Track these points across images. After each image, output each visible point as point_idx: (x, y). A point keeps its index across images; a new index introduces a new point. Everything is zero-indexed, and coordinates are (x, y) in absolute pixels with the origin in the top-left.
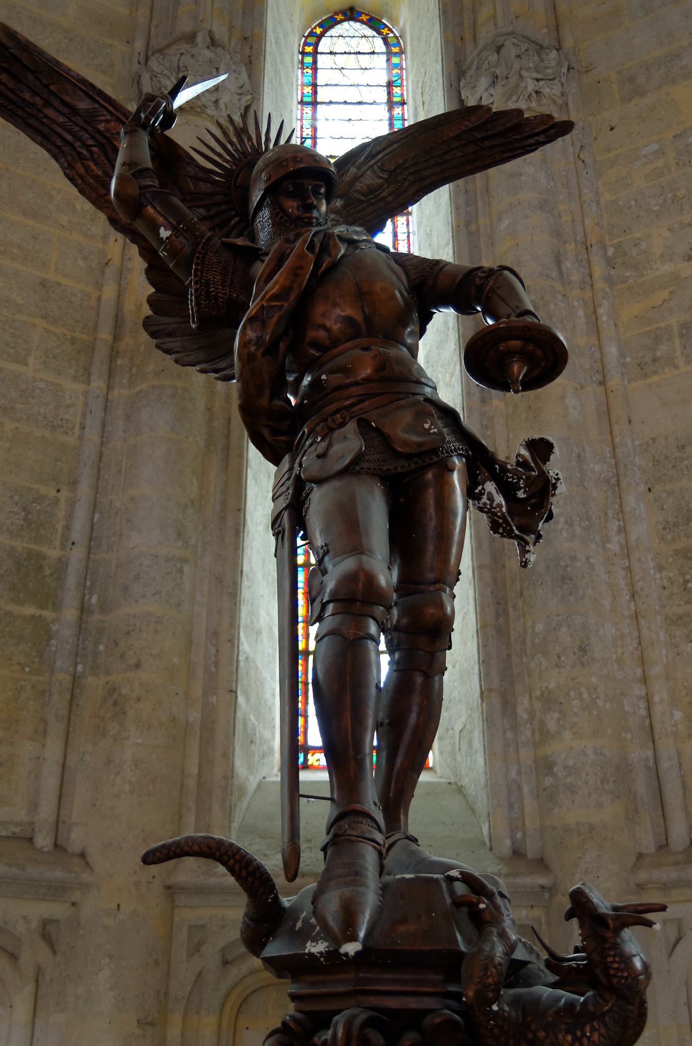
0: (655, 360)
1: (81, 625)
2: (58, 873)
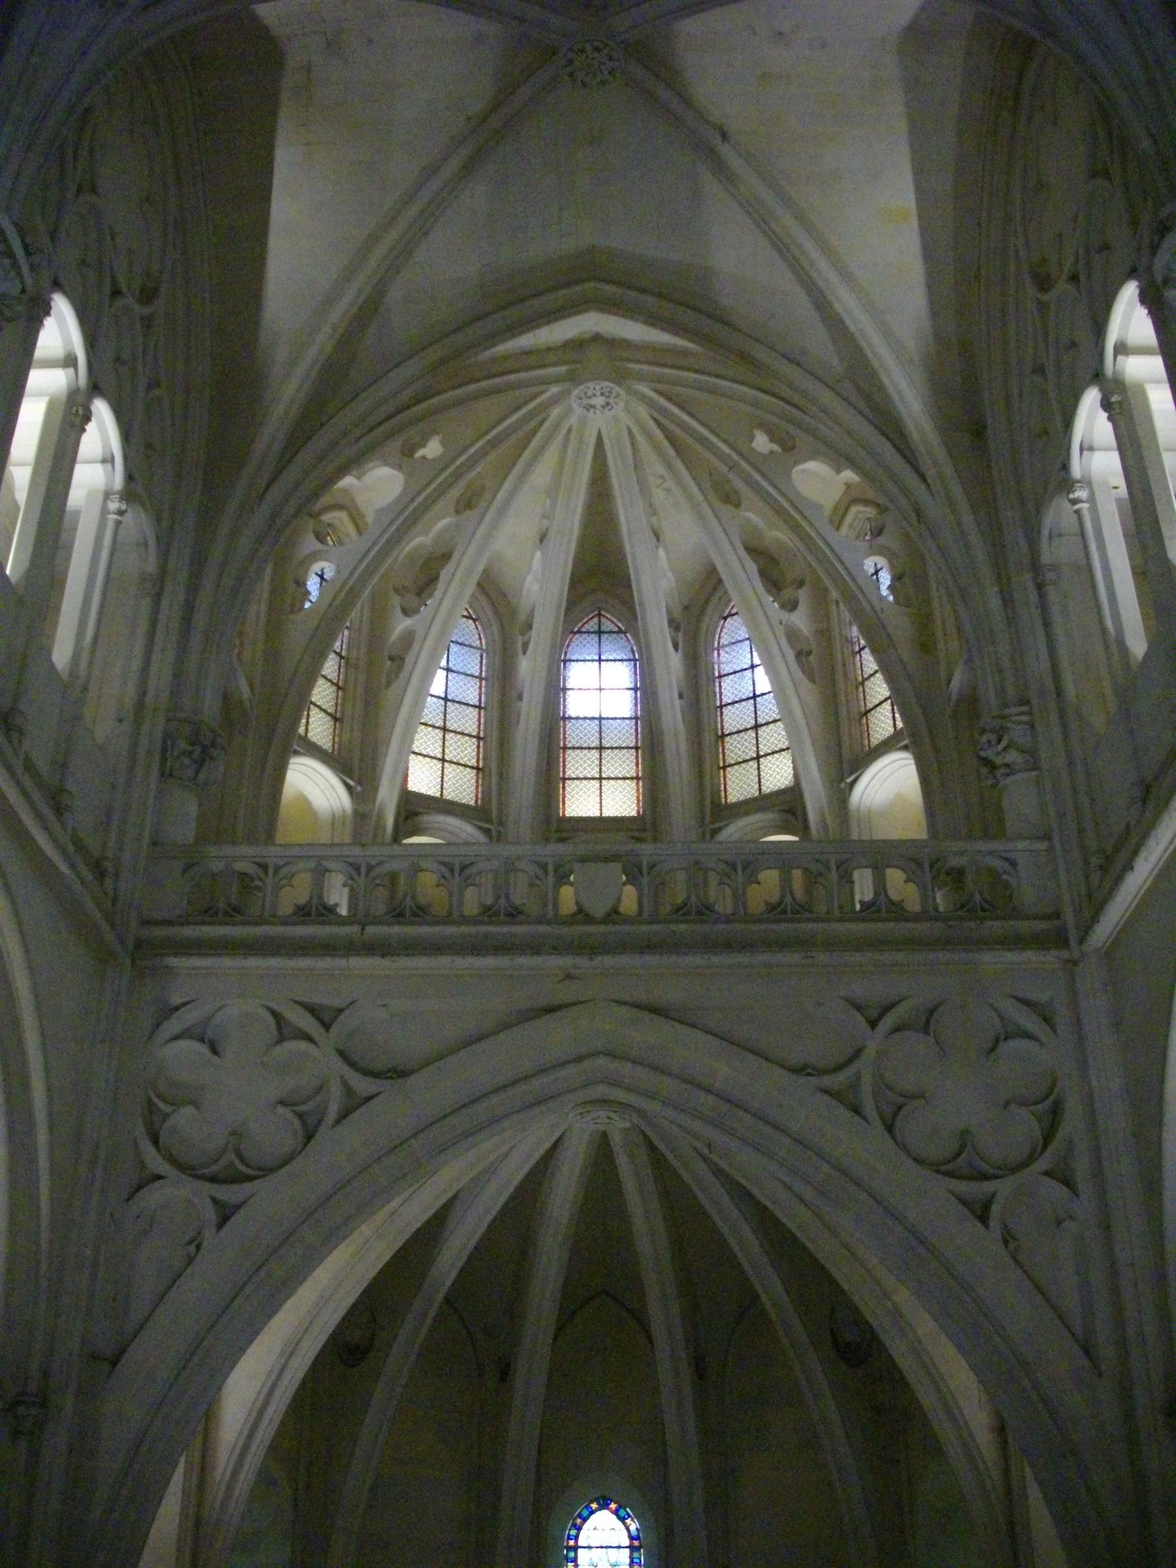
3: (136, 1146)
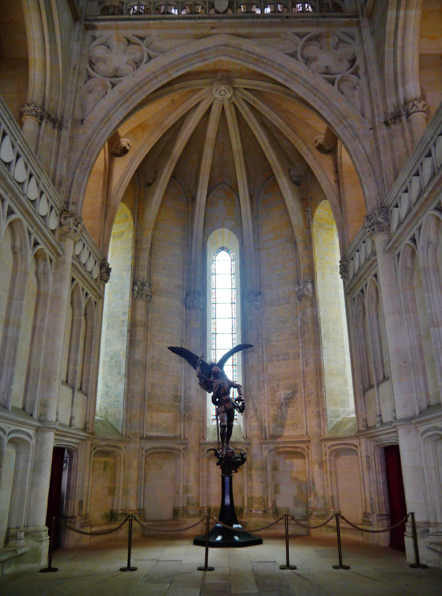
1: (185, 406)
2: (185, 442)
3: (87, 70)
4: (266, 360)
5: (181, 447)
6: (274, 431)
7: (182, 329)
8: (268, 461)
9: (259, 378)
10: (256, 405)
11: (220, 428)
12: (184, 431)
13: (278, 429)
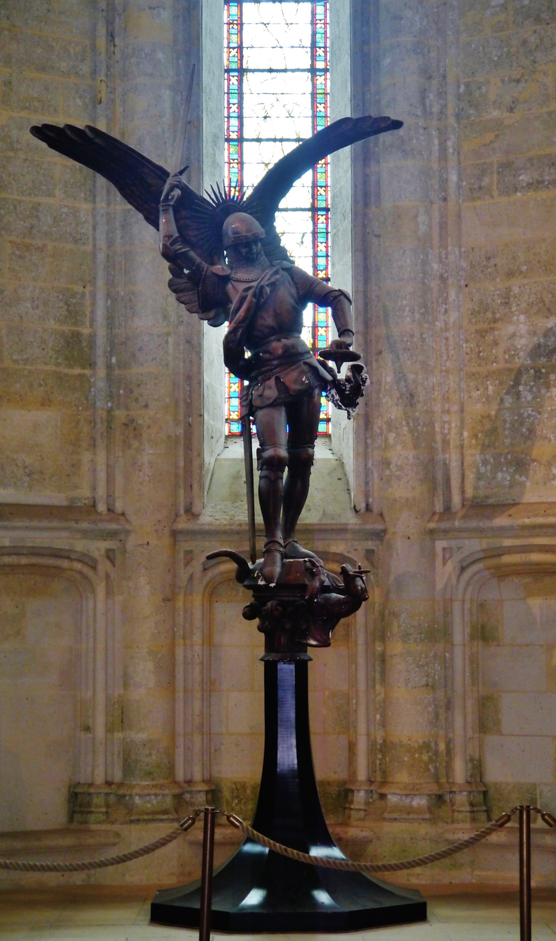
0: (480, 188)
1: (109, 378)
2: (114, 526)
4: (459, 187)
5: (98, 548)
6: (481, 483)
7: (94, 48)
8: (457, 606)
9: (425, 263)
10: (411, 377)
11: (260, 468)
12: (110, 481)
13: (500, 475)
